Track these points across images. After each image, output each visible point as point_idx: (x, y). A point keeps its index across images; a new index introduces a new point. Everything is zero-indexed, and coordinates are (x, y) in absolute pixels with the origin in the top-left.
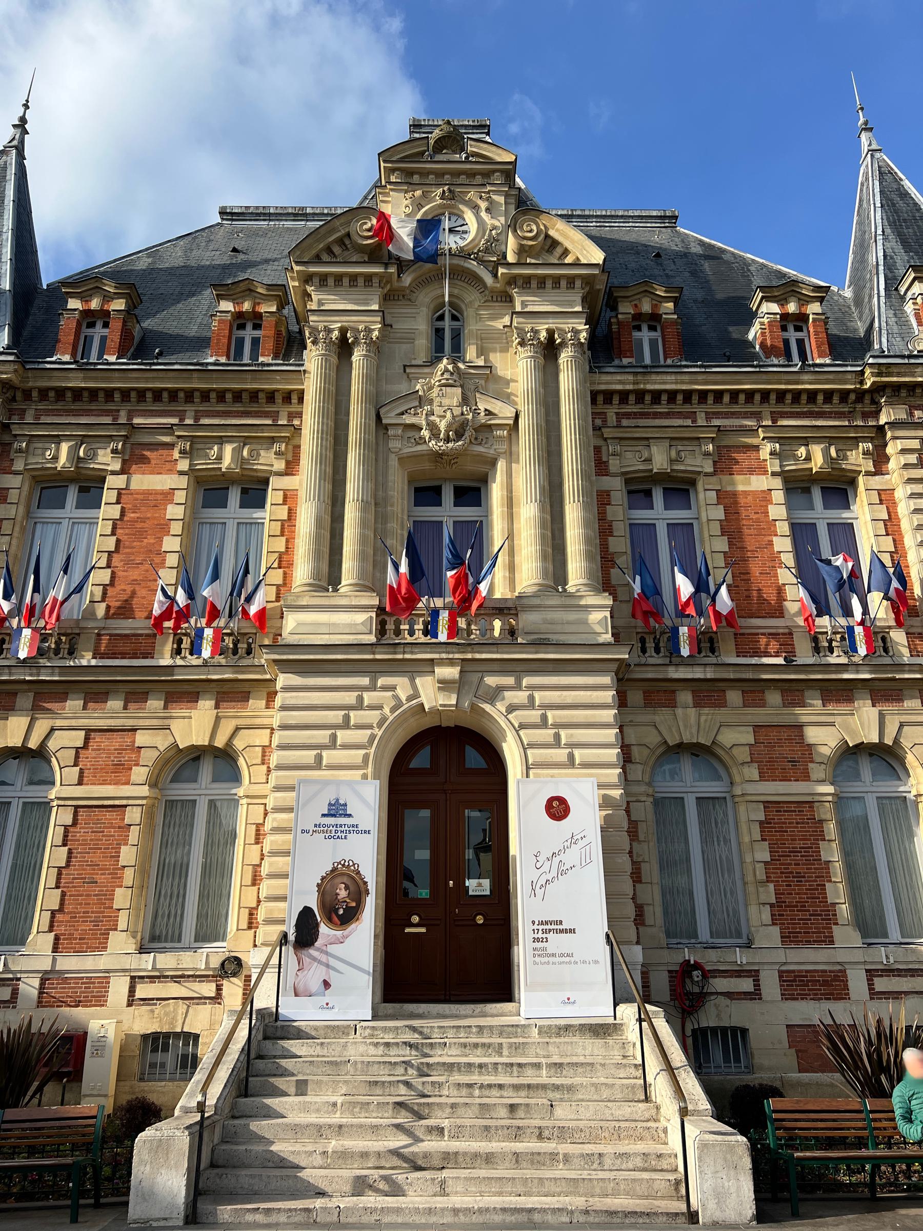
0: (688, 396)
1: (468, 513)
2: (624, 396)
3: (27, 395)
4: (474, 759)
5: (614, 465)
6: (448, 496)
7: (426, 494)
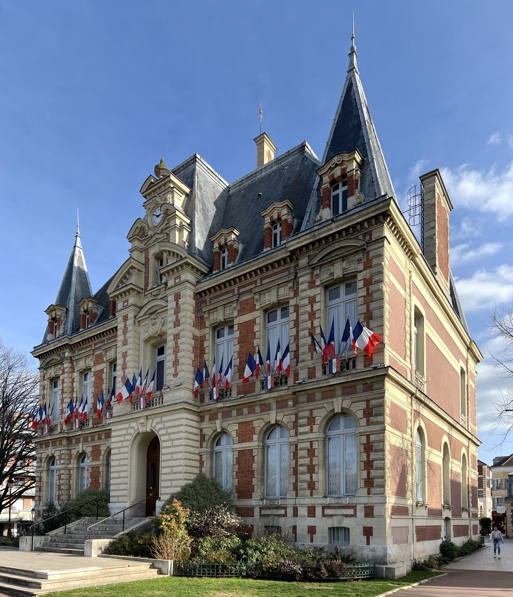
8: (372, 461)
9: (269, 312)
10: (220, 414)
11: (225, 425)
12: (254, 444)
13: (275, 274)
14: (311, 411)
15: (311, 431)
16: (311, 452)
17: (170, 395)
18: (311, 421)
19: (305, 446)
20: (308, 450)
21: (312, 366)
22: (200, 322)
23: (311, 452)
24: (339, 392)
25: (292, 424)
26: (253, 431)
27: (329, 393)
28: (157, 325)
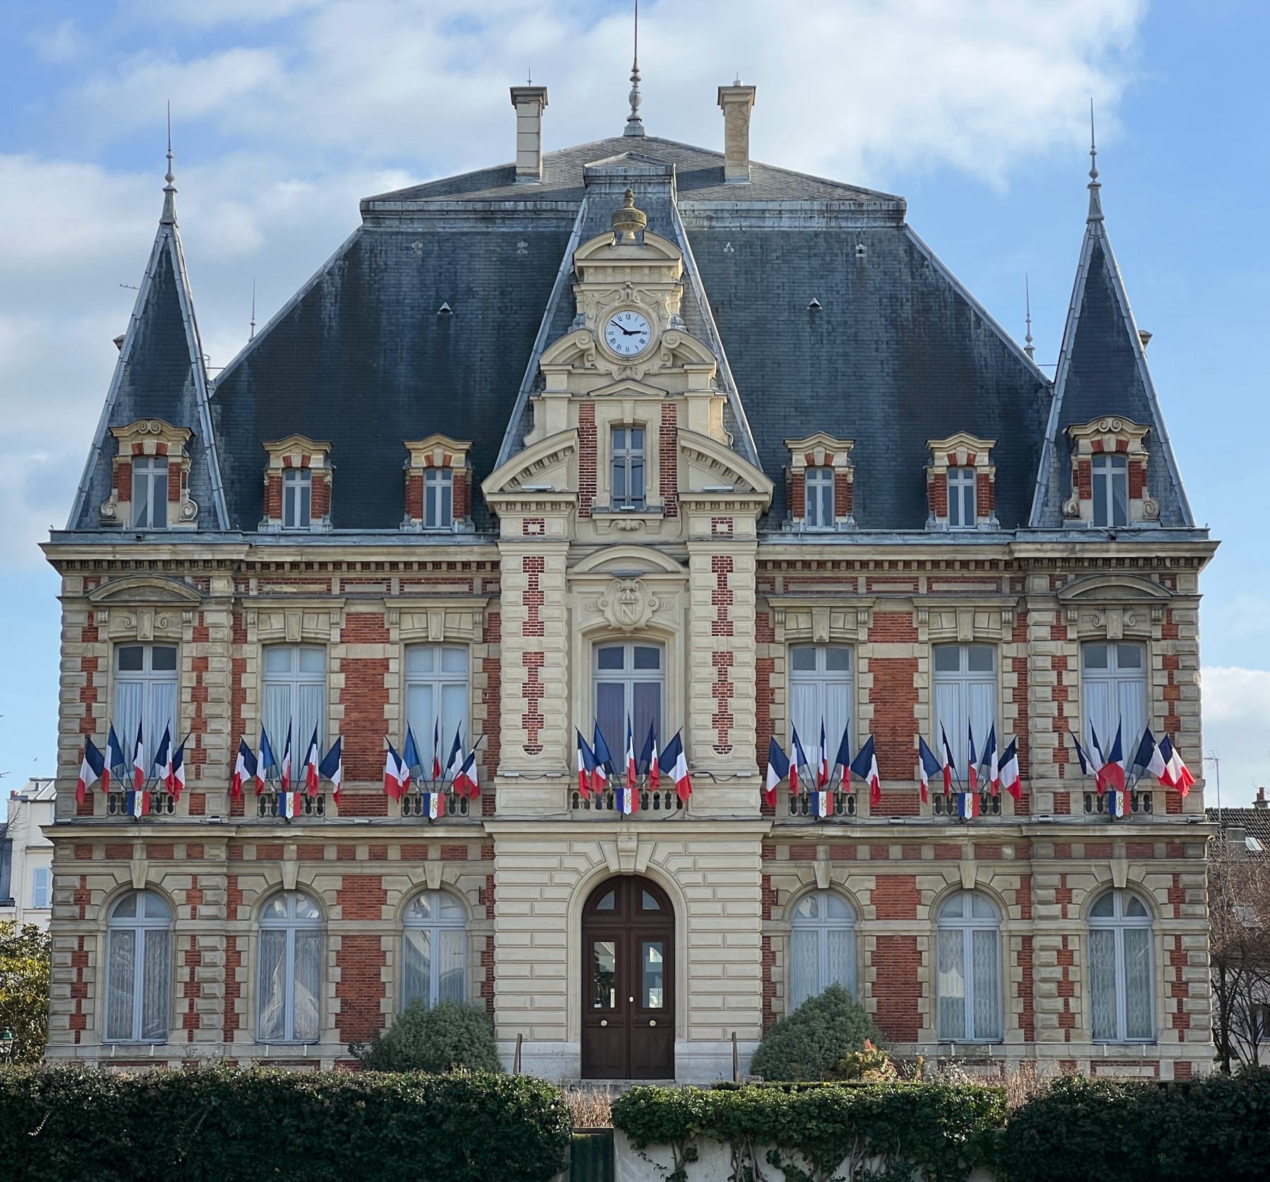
0: (850, 564)
1: (647, 675)
2: (792, 564)
3: (251, 565)
4: (649, 903)
5: (780, 635)
6: (629, 657)
7: (609, 657)
8: (1186, 983)
9: (945, 654)
10: (821, 849)
11: (839, 875)
12: (919, 925)
13: (965, 580)
14: (1064, 876)
15: (1065, 915)
16: (1065, 957)
17: (713, 793)
18: (1064, 896)
19: (1053, 944)
20: (1059, 952)
21: (1062, 790)
22: (764, 632)
23: (1065, 957)
24: (1120, 850)
25: (1013, 895)
26: (915, 898)
27: (1100, 849)
28: (639, 608)
